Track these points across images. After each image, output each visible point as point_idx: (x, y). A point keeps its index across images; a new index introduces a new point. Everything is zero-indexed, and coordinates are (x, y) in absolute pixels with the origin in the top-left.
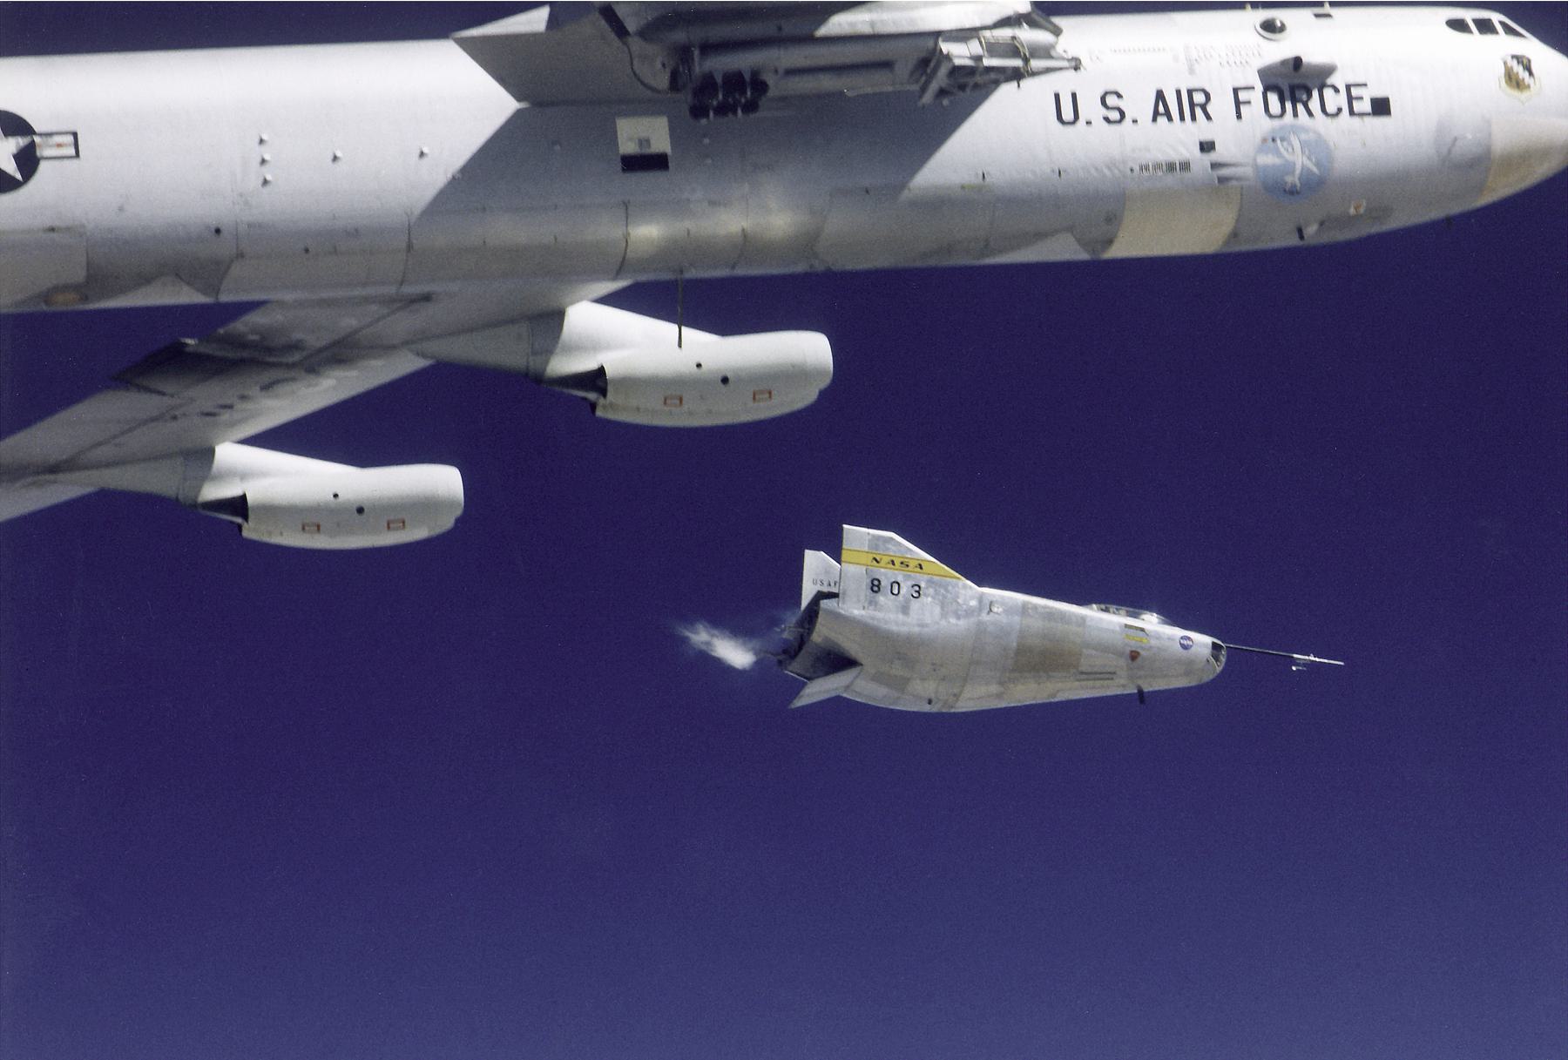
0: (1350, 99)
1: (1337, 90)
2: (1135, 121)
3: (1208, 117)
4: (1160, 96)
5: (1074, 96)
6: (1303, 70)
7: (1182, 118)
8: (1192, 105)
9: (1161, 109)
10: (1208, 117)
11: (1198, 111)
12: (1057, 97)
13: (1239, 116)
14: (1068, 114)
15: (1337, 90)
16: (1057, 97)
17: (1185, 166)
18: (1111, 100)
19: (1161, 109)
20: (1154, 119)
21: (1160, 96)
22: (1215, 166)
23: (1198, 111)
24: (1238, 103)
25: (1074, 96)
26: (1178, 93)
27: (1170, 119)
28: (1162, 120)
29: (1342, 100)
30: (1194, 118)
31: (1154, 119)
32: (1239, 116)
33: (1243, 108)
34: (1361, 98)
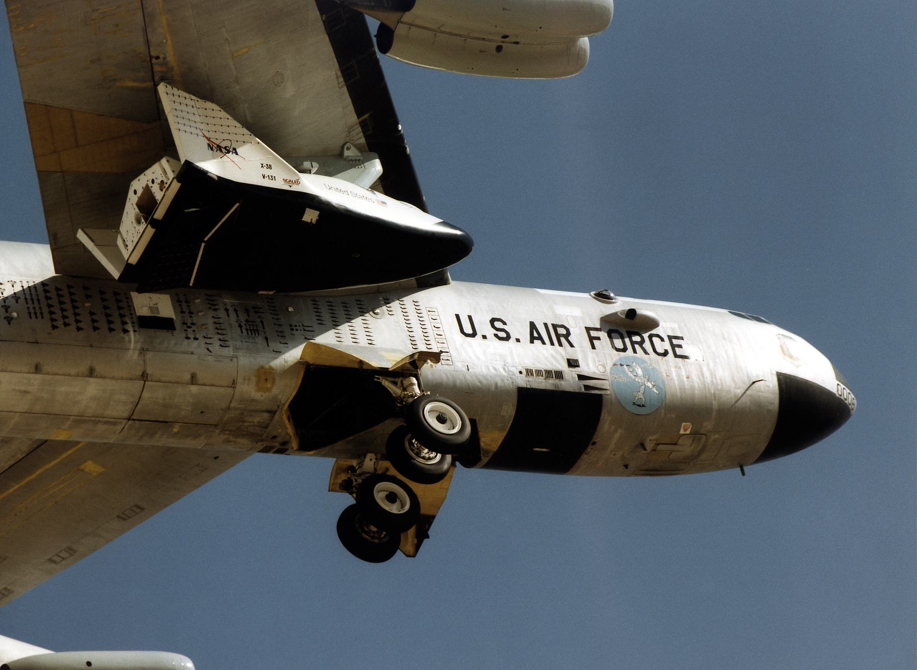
0: (673, 347)
1: (662, 340)
2: (518, 340)
3: (572, 346)
4: (533, 326)
5: (470, 317)
6: (637, 320)
7: (552, 344)
8: (558, 336)
9: (535, 335)
10: (572, 346)
11: (563, 340)
12: (458, 316)
13: (593, 347)
14: (468, 330)
15: (662, 340)
16: (458, 316)
17: (559, 375)
18: (498, 325)
19: (535, 335)
20: (532, 342)
21: (533, 326)
22: (581, 377)
23: (563, 340)
24: (592, 339)
25: (470, 317)
26: (546, 325)
27: (544, 343)
28: (537, 343)
29: (667, 345)
30: (560, 344)
31: (532, 342)
32: (593, 347)
33: (595, 342)
34: (680, 346)
